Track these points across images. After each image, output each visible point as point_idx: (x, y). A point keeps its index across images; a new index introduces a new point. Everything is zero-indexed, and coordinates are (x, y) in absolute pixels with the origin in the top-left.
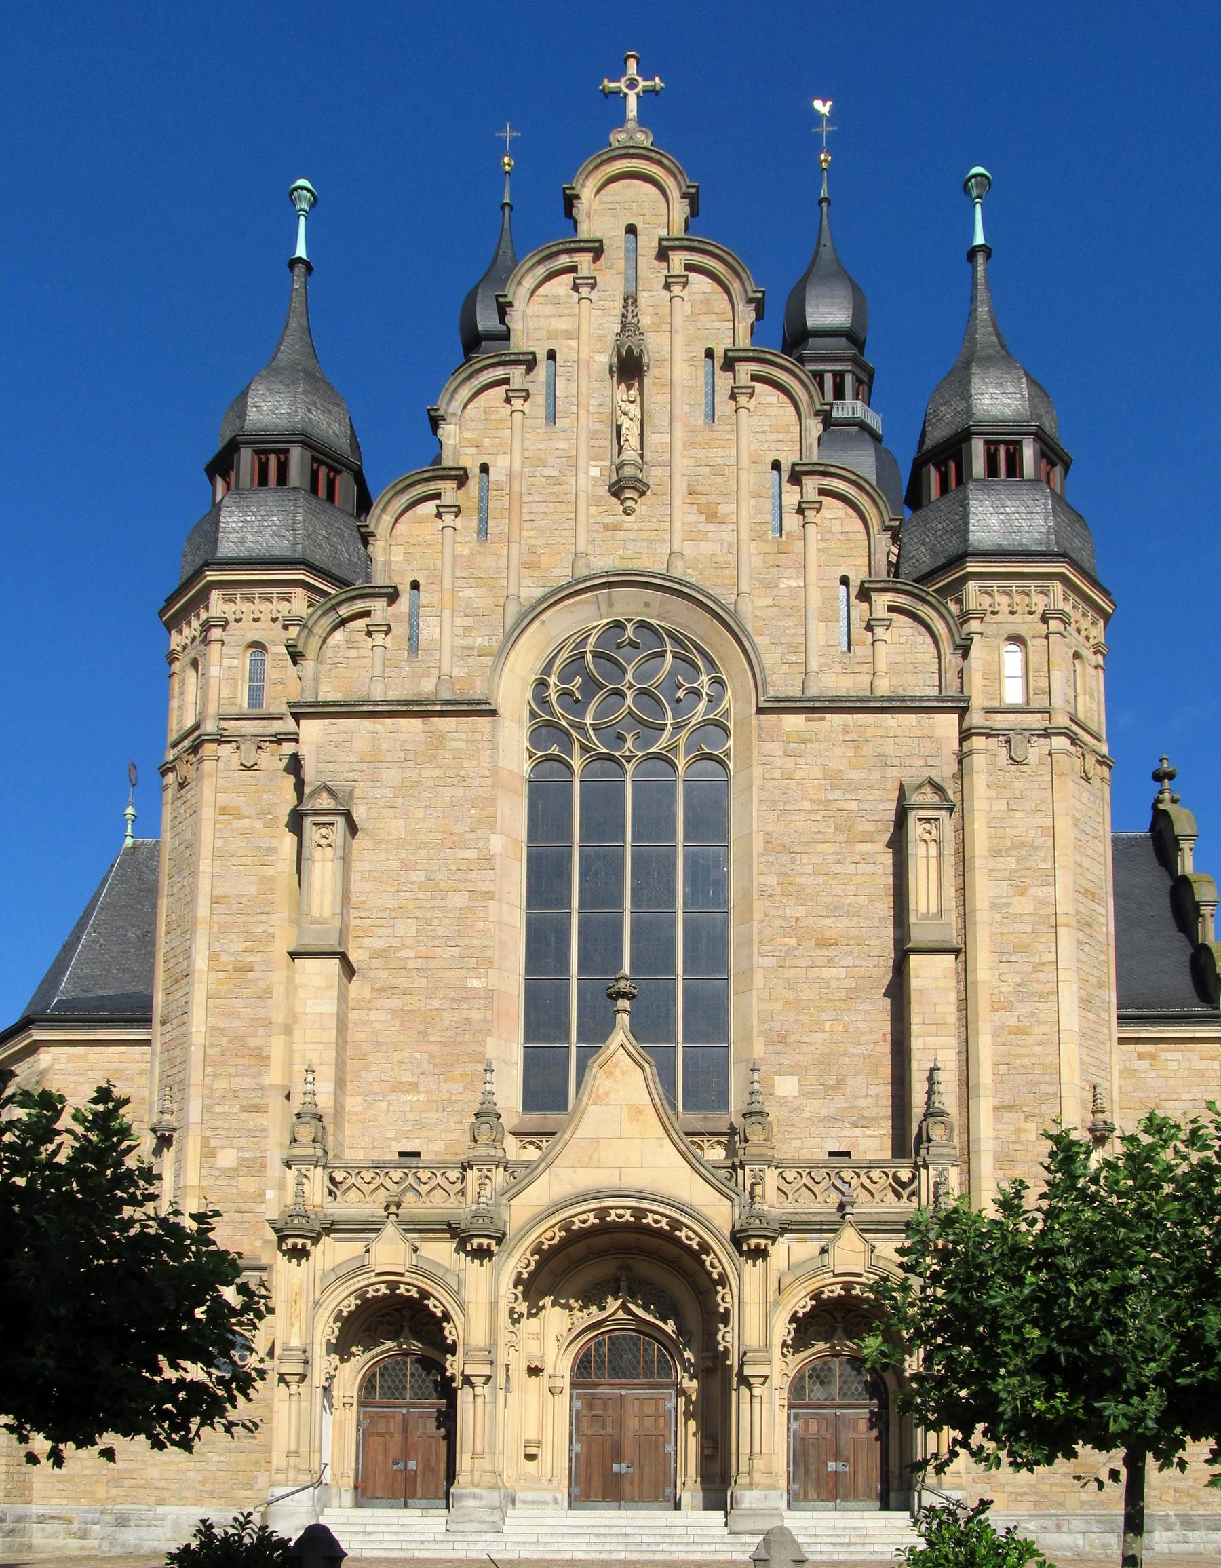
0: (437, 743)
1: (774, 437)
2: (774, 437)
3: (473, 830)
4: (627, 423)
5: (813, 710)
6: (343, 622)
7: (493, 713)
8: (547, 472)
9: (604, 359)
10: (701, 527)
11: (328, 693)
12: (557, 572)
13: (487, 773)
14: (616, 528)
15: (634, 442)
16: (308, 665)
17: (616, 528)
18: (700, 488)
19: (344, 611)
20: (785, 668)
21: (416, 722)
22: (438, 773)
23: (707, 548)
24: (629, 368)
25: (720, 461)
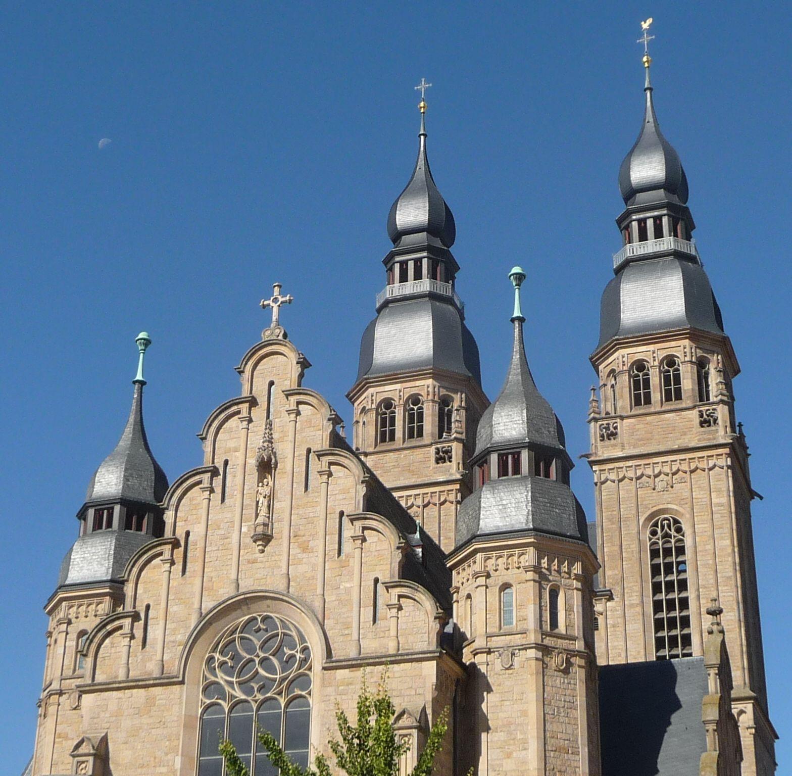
0: (150, 702)
1: (341, 497)
2: (341, 497)
3: (167, 754)
4: (261, 499)
5: (352, 666)
6: (109, 634)
7: (182, 683)
8: (221, 532)
9: (252, 462)
10: (299, 556)
11: (100, 678)
12: (221, 591)
13: (175, 719)
14: (254, 561)
15: (263, 511)
16: (90, 660)
17: (254, 561)
18: (301, 533)
19: (109, 627)
20: (341, 639)
21: (142, 690)
22: (151, 721)
23: (302, 568)
24: (266, 467)
25: (311, 515)
